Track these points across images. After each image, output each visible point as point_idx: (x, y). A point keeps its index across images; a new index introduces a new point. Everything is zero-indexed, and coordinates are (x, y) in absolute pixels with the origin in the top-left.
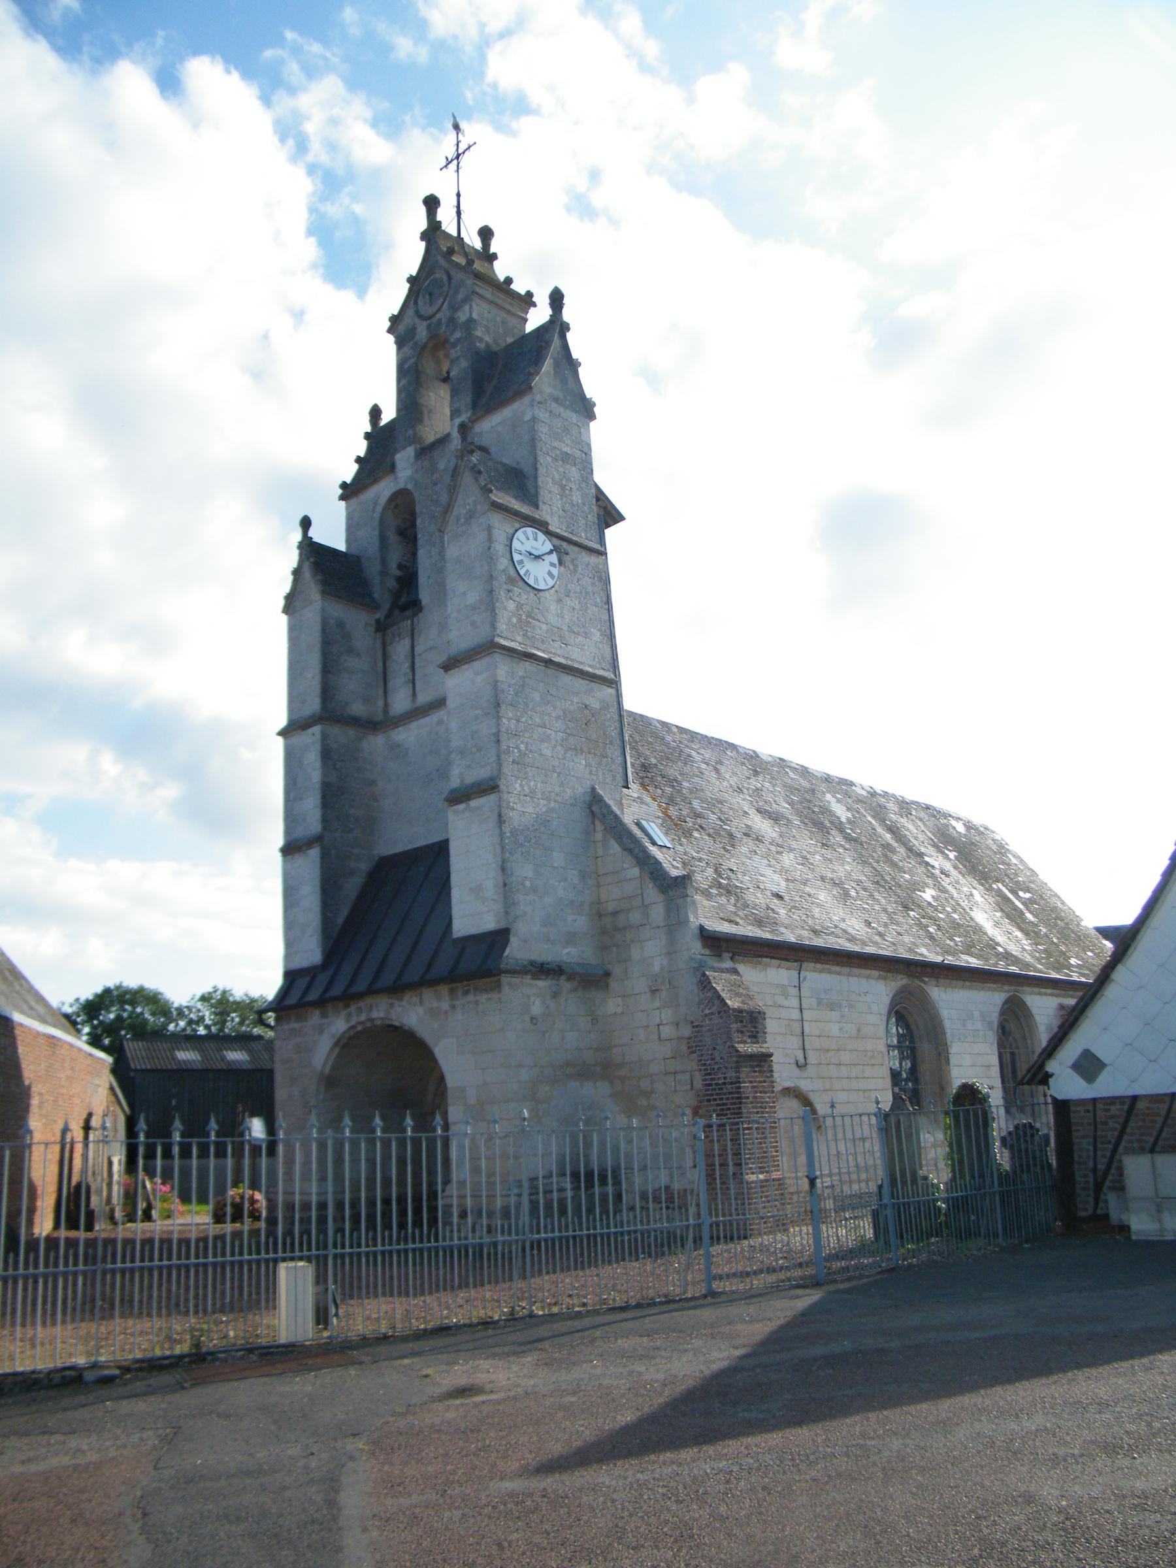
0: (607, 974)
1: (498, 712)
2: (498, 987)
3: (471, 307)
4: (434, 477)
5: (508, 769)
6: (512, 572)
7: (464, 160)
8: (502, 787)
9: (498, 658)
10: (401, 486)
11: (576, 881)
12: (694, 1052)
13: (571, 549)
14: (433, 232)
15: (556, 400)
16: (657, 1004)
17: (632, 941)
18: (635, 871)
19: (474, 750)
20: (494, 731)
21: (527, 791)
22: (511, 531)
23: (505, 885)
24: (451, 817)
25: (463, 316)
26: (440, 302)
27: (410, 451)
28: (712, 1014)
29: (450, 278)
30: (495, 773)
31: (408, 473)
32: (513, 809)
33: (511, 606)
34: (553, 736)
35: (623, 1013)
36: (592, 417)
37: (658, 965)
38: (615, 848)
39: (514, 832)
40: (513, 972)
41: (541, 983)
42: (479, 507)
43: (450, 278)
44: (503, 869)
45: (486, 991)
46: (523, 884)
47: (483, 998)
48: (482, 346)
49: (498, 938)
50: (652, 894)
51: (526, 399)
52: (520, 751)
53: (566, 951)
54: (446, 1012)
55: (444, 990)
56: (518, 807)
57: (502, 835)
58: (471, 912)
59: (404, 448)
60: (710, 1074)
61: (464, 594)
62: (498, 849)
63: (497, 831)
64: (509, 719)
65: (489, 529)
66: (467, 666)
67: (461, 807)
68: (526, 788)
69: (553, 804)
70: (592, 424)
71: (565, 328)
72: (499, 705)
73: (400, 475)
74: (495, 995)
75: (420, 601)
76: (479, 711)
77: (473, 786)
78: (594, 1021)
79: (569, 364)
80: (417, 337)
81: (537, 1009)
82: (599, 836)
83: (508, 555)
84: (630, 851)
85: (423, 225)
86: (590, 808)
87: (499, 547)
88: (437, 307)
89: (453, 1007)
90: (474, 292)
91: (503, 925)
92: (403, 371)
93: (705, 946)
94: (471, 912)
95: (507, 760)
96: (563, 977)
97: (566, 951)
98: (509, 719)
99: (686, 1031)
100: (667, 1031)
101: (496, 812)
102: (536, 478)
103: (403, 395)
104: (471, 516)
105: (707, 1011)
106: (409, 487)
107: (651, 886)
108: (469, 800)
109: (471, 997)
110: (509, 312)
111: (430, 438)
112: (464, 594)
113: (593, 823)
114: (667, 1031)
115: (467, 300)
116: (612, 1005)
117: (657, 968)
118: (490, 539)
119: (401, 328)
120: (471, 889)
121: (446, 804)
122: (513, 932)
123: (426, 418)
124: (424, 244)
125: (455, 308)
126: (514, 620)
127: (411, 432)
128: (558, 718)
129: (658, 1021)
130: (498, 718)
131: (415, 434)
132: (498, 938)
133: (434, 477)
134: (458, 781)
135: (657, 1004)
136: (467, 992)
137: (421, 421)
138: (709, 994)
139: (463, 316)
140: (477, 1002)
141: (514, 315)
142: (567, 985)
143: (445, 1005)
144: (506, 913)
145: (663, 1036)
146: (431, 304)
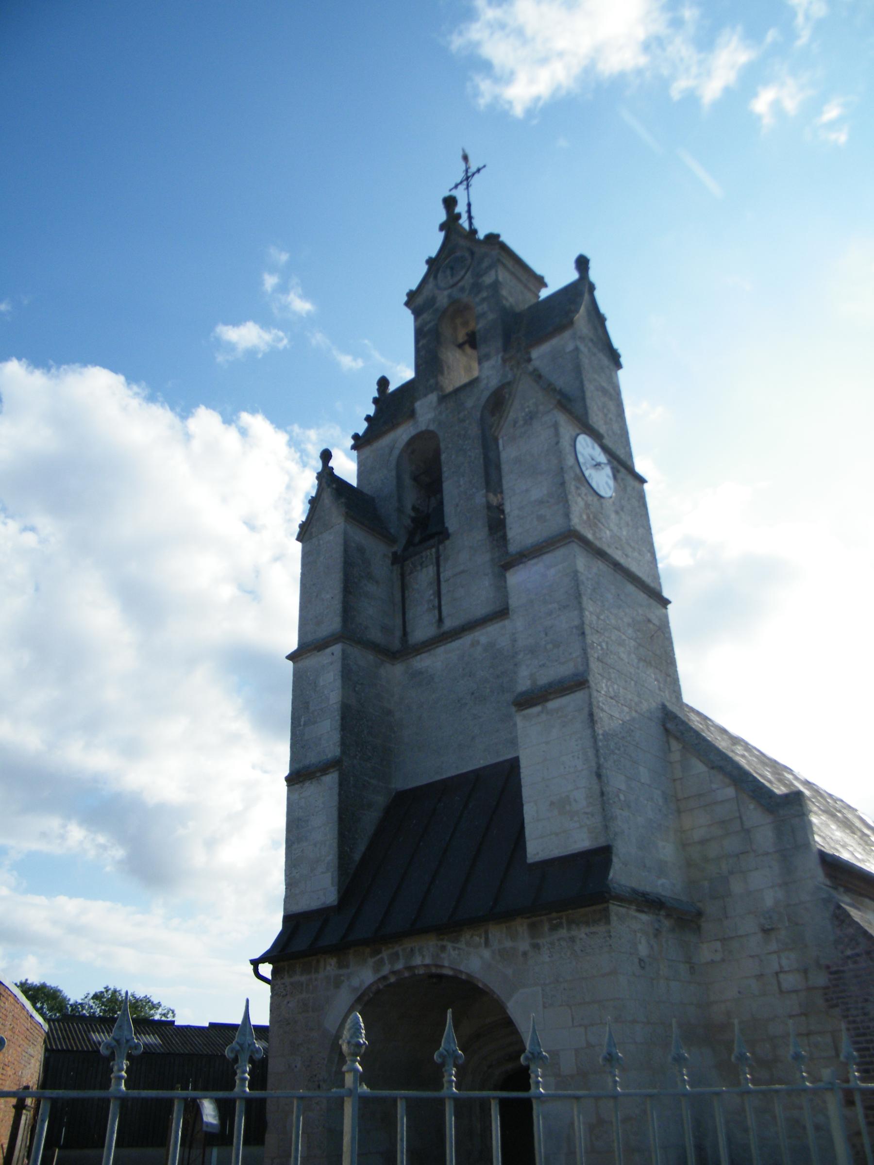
0: (700, 914)
1: (580, 603)
2: (605, 917)
3: (497, 271)
4: (461, 415)
5: (594, 666)
6: (578, 471)
7: (474, 181)
8: (592, 684)
9: (575, 548)
10: (422, 427)
11: (661, 802)
12: (836, 1006)
13: (622, 470)
14: (450, 225)
15: (592, 340)
16: (774, 946)
17: (731, 873)
18: (730, 792)
19: (550, 646)
20: (576, 623)
21: (612, 694)
22: (574, 434)
23: (602, 794)
24: (519, 720)
25: (488, 279)
26: (462, 273)
27: (433, 398)
28: (858, 955)
29: (472, 253)
30: (581, 668)
31: (431, 415)
32: (602, 710)
33: (582, 504)
34: (627, 642)
35: (723, 960)
36: (619, 366)
37: (769, 899)
38: (699, 767)
39: (605, 734)
40: (620, 899)
41: (644, 917)
42: (541, 408)
43: (472, 253)
44: (599, 776)
45: (587, 924)
46: (618, 796)
47: (581, 933)
48: (507, 304)
49: (598, 859)
50: (754, 815)
51: (567, 334)
52: (602, 649)
53: (660, 882)
54: (525, 954)
55: (521, 926)
56: (606, 708)
57: (594, 737)
58: (550, 830)
59: (425, 395)
60: (864, 1034)
61: (527, 491)
62: (591, 753)
63: (589, 731)
64: (591, 613)
65: (556, 426)
66: (535, 560)
67: (537, 709)
68: (611, 689)
69: (634, 714)
70: (621, 373)
71: (592, 288)
72: (580, 595)
73: (420, 419)
74: (601, 929)
75: (447, 529)
76: (556, 605)
77: (550, 685)
78: (692, 969)
79: (598, 319)
80: (438, 304)
81: (643, 950)
82: (676, 756)
83: (573, 454)
84: (721, 769)
85: (442, 216)
86: (664, 726)
87: (565, 443)
88: (459, 277)
89: (536, 947)
90: (499, 260)
91: (601, 842)
92: (420, 334)
93: (828, 875)
94: (550, 830)
95: (594, 654)
96: (663, 913)
97: (660, 882)
98: (591, 613)
99: (820, 979)
100: (790, 981)
101: (586, 711)
102: (584, 399)
103: (423, 353)
104: (530, 418)
105: (849, 952)
106: (432, 427)
107: (752, 806)
108: (547, 700)
109: (563, 932)
110: (526, 286)
111: (449, 389)
112: (527, 491)
113: (668, 742)
114: (790, 981)
115: (490, 268)
116: (707, 952)
117: (769, 902)
118: (557, 434)
119: (420, 300)
120: (552, 803)
121: (514, 709)
122: (614, 850)
123: (446, 372)
124: (442, 235)
125: (478, 275)
126: (585, 517)
127: (432, 381)
128: (629, 625)
129: (776, 967)
130: (581, 610)
131: (437, 383)
132: (598, 859)
133: (461, 415)
134: (529, 683)
135: (774, 946)
136: (554, 928)
137: (442, 373)
138: (851, 930)
139: (488, 279)
140: (573, 940)
141: (529, 290)
142: (667, 923)
143: (524, 945)
144: (606, 827)
145: (785, 986)
146: (452, 275)
